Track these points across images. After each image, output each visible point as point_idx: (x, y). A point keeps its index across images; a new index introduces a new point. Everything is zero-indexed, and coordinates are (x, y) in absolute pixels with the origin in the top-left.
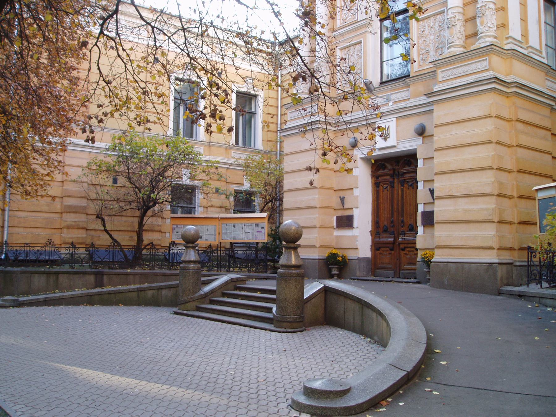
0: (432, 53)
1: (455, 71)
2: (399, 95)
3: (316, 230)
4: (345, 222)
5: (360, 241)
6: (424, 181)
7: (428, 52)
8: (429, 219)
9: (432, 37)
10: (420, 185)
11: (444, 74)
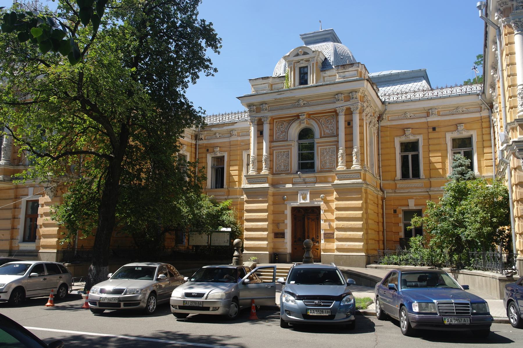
7: (326, 163)
10: (322, 222)
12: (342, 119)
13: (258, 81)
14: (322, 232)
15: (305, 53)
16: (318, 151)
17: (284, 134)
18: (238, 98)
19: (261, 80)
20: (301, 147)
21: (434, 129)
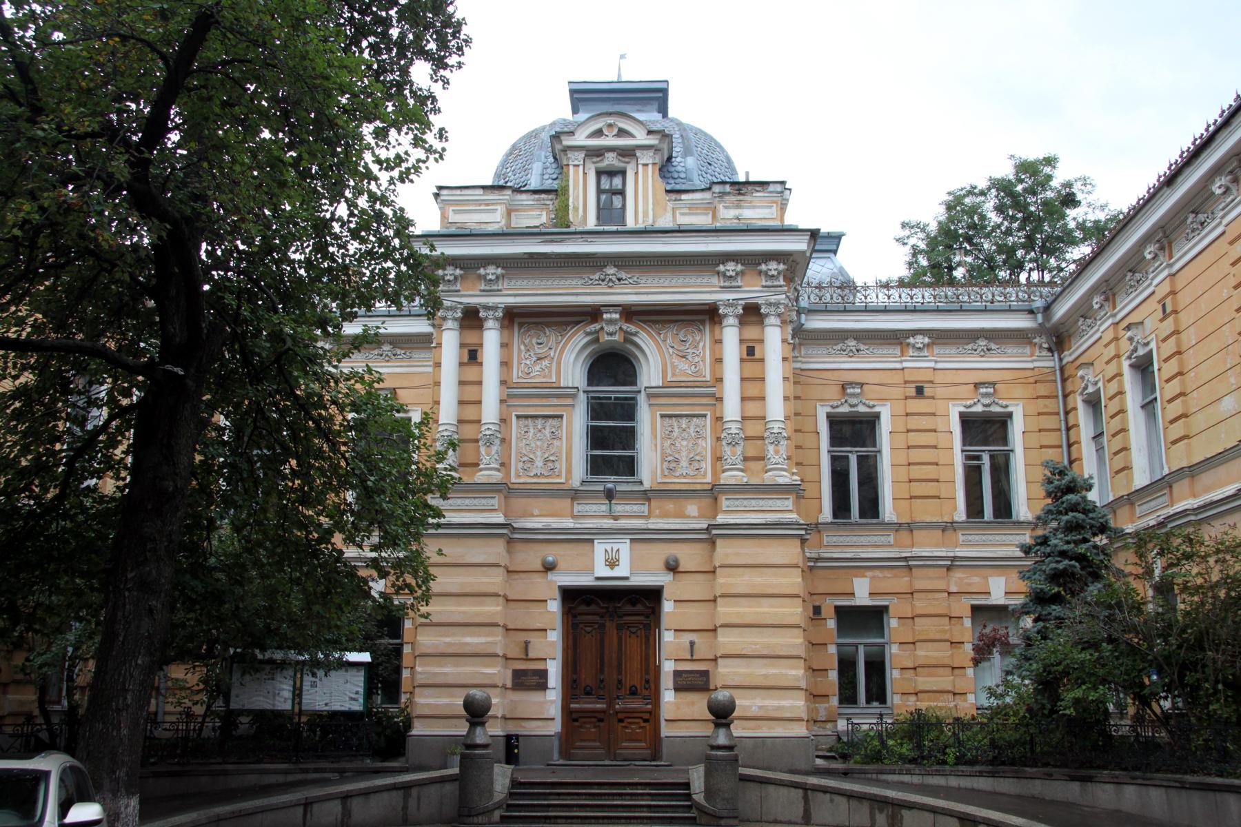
0: (684, 463)
1: (745, 502)
2: (628, 508)
4: (529, 680)
5: (546, 709)
7: (677, 461)
9: (684, 443)
10: (668, 637)
11: (728, 503)
12: (731, 335)
14: (668, 667)
15: (622, 133)
16: (646, 421)
17: (545, 363)
19: (481, 191)
20: (598, 409)
21: (920, 391)
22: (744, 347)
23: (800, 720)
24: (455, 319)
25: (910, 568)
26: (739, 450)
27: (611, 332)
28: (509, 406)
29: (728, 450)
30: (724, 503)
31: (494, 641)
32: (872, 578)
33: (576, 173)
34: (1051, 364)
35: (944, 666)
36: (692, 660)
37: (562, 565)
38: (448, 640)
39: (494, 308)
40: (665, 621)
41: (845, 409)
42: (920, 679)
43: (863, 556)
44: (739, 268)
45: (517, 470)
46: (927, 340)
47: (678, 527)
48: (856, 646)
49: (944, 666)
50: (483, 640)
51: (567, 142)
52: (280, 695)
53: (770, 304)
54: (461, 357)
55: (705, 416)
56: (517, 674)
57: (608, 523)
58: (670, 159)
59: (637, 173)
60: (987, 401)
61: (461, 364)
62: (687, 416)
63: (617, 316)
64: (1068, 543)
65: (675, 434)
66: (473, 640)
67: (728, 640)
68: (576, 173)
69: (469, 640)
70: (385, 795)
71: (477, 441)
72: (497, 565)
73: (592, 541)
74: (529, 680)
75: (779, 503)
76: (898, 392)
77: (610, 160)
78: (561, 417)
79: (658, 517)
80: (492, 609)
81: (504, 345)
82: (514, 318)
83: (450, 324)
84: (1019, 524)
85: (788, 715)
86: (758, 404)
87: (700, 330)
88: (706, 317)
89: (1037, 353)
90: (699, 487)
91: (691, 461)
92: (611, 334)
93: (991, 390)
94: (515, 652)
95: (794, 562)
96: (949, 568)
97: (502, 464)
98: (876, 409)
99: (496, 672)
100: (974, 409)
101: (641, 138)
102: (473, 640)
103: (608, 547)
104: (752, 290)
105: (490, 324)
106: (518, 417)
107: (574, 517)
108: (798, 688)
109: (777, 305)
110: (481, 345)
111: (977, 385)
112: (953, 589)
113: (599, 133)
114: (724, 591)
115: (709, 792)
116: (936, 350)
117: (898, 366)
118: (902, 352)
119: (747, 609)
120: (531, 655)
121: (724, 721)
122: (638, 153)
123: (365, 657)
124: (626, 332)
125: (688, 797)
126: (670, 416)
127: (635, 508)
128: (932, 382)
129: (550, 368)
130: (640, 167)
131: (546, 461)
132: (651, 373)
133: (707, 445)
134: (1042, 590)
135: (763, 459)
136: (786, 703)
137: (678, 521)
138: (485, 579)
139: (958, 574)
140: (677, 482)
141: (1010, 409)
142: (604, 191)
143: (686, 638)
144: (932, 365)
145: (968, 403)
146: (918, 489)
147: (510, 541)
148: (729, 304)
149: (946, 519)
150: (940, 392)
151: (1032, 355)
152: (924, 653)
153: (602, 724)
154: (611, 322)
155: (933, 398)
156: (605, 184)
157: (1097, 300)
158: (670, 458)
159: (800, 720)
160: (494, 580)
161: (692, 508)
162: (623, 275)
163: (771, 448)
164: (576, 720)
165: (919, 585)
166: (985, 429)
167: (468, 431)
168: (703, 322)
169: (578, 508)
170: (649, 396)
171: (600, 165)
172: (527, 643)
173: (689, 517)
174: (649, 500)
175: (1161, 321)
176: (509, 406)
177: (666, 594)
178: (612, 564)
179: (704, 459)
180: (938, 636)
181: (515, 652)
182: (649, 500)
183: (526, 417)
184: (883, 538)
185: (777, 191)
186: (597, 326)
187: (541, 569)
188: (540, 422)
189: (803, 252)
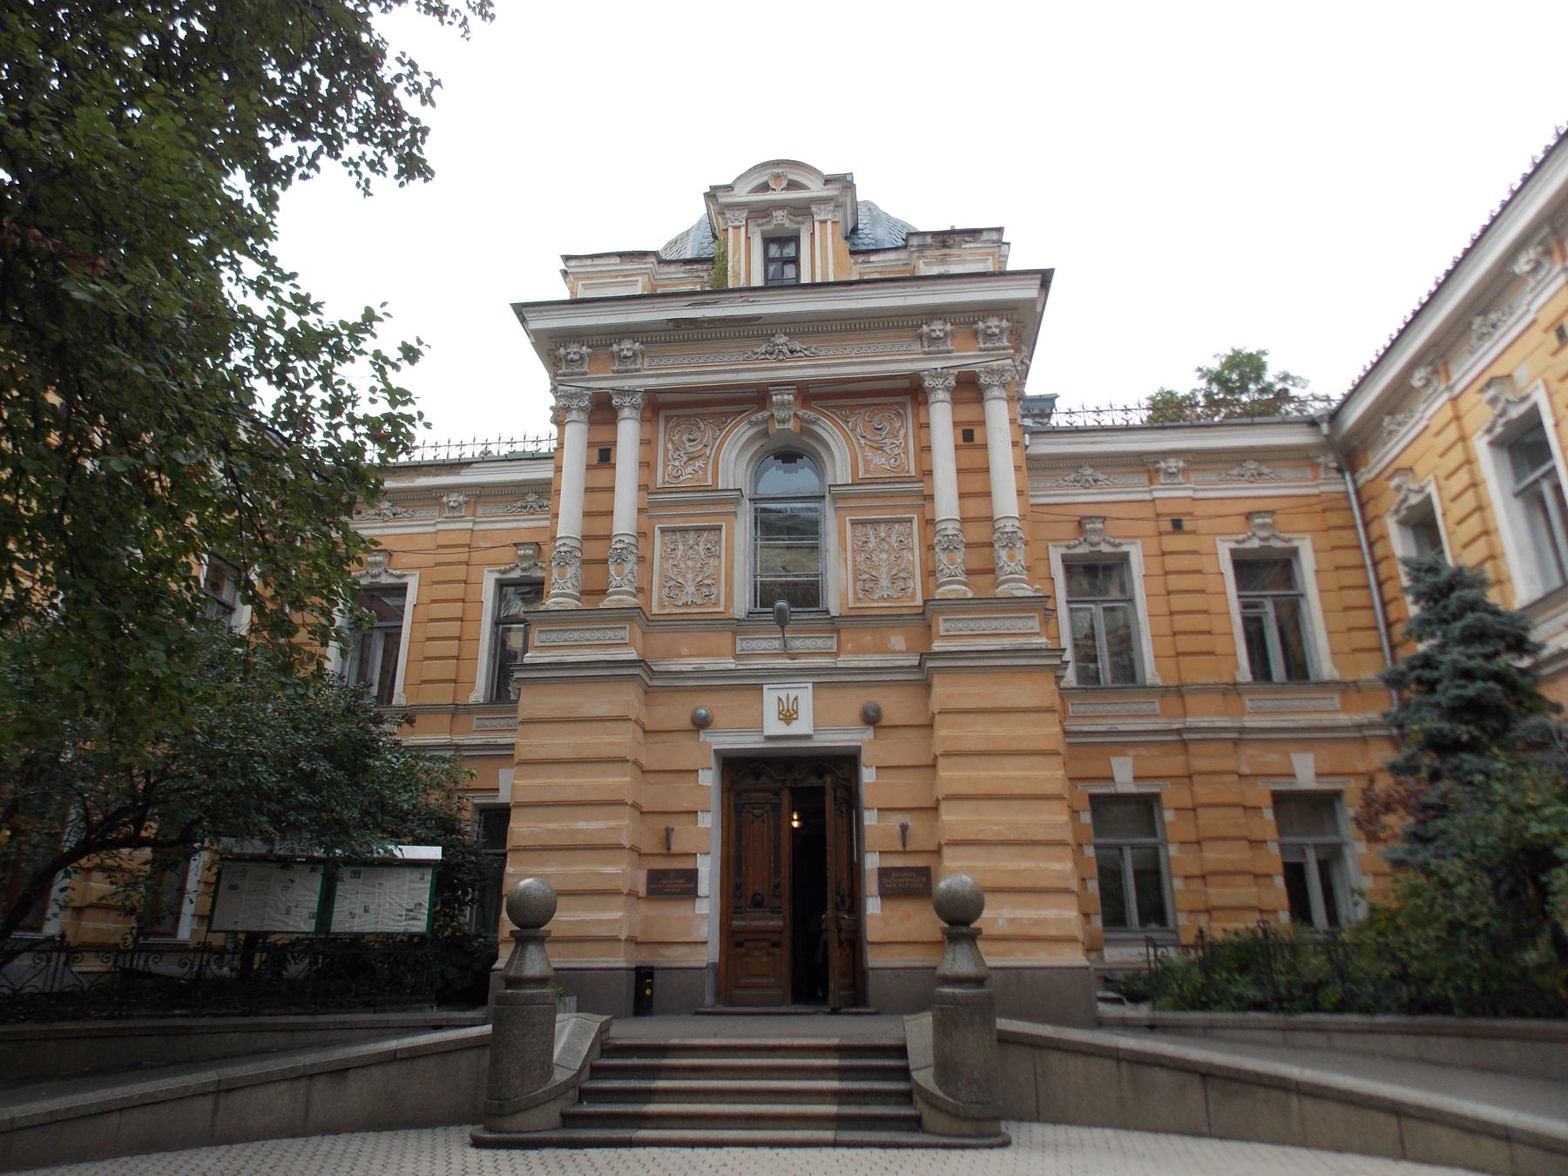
0: (885, 582)
1: (972, 624)
2: (809, 643)
3: (621, 900)
4: (672, 884)
5: (698, 927)
6: (879, 809)
7: (875, 580)
8: (910, 884)
9: (884, 556)
10: (870, 819)
11: (948, 625)
12: (941, 416)
13: (597, 261)
14: (872, 862)
15: (793, 185)
17: (699, 463)
18: (522, 311)
19: (617, 260)
21: (1177, 525)
22: (960, 431)
23: (1071, 940)
24: (581, 409)
25: (1184, 743)
26: (959, 556)
27: (786, 417)
28: (650, 517)
29: (943, 557)
30: (942, 626)
31: (620, 827)
32: (1136, 757)
33: (737, 236)
34: (1341, 488)
35: (1243, 873)
36: (905, 852)
37: (718, 720)
38: (552, 826)
39: (631, 392)
40: (866, 796)
41: (1082, 550)
42: (1212, 891)
43: (1121, 728)
44: (949, 327)
45: (660, 598)
46: (1181, 464)
47: (878, 664)
48: (1120, 848)
49: (1243, 873)
50: (601, 825)
51: (724, 199)
52: (292, 911)
53: (991, 372)
54: (588, 457)
55: (910, 520)
56: (655, 877)
57: (786, 663)
58: (855, 230)
59: (813, 234)
60: (1264, 534)
61: (589, 467)
62: (886, 521)
63: (791, 397)
64: (1470, 657)
65: (872, 544)
66: (590, 826)
67: (954, 819)
68: (737, 236)
69: (582, 825)
70: (377, 1072)
71: (605, 561)
72: (625, 719)
73: (760, 688)
74: (672, 884)
75: (1020, 623)
76: (1149, 528)
77: (780, 217)
78: (719, 529)
79: (850, 652)
80: (617, 781)
81: (646, 442)
82: (656, 406)
83: (574, 415)
84: (1325, 685)
85: (1053, 932)
86: (981, 501)
87: (899, 415)
88: (907, 399)
89: (1322, 475)
90: (905, 611)
91: (894, 579)
92: (783, 421)
93: (1268, 520)
94: (650, 844)
95: (1047, 703)
96: (1236, 742)
97: (640, 590)
98: (1124, 549)
99: (618, 871)
100: (1248, 545)
101: (816, 190)
102: (590, 826)
103: (783, 695)
104: (967, 357)
105: (626, 412)
106: (663, 531)
107: (736, 657)
108: (1066, 891)
109: (1001, 372)
110: (615, 443)
111: (1249, 516)
112: (1245, 770)
113: (765, 187)
114: (948, 747)
115: (945, 1068)
116: (1193, 477)
117: (1147, 497)
118: (1151, 482)
119: (983, 774)
120: (675, 849)
121: (965, 930)
122: (814, 209)
123: (434, 853)
124: (802, 420)
125: (904, 1073)
126: (864, 523)
127: (820, 643)
128: (1190, 514)
129: (705, 470)
130: (817, 225)
131: (699, 585)
132: (840, 470)
133: (915, 557)
134: (1440, 730)
135: (992, 571)
136: (1049, 914)
137: (877, 657)
138: (607, 739)
139: (1249, 751)
140: (873, 604)
141: (1295, 543)
142: (774, 260)
143: (896, 820)
144: (1190, 493)
145: (1241, 537)
146: (1185, 644)
147: (649, 691)
148: (936, 374)
149: (1226, 680)
150: (1202, 525)
151: (1315, 478)
152: (1214, 855)
153: (777, 950)
154: (783, 404)
155: (1193, 532)
156: (774, 251)
157: (1417, 380)
158: (865, 576)
159: (1071, 940)
160: (620, 740)
161: (898, 641)
162: (797, 346)
163: (1003, 554)
164: (739, 945)
165: (1199, 764)
166: (1264, 571)
167: (595, 550)
168: (903, 405)
169: (741, 645)
170: (835, 498)
171: (765, 228)
172: (668, 832)
173: (894, 652)
174: (838, 631)
175: (1555, 353)
176: (650, 517)
177: (865, 757)
178: (788, 717)
179: (912, 576)
180: (1231, 832)
181: (650, 844)
182: (838, 631)
183: (674, 530)
184: (1145, 707)
185: (991, 238)
186: (766, 414)
187: (691, 727)
188: (691, 537)
189: (1033, 302)
